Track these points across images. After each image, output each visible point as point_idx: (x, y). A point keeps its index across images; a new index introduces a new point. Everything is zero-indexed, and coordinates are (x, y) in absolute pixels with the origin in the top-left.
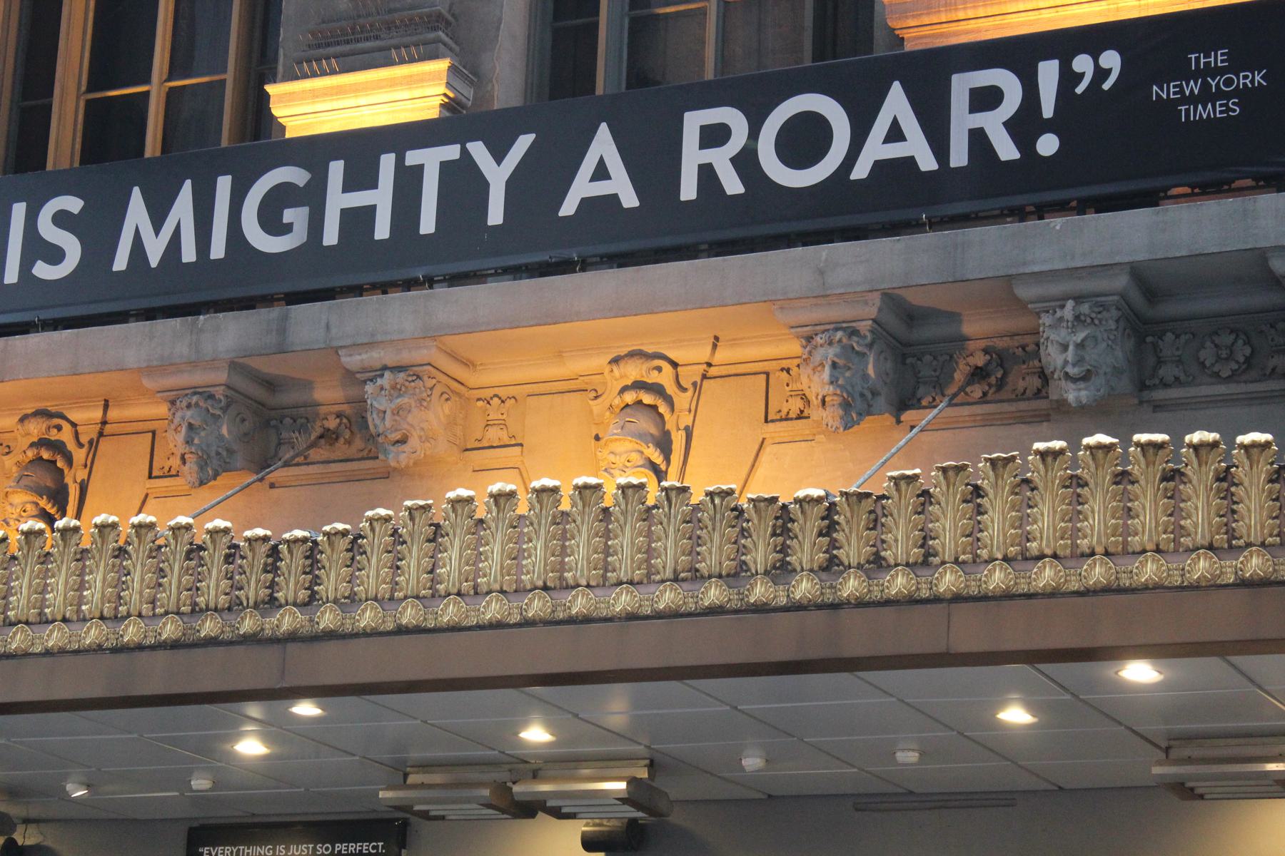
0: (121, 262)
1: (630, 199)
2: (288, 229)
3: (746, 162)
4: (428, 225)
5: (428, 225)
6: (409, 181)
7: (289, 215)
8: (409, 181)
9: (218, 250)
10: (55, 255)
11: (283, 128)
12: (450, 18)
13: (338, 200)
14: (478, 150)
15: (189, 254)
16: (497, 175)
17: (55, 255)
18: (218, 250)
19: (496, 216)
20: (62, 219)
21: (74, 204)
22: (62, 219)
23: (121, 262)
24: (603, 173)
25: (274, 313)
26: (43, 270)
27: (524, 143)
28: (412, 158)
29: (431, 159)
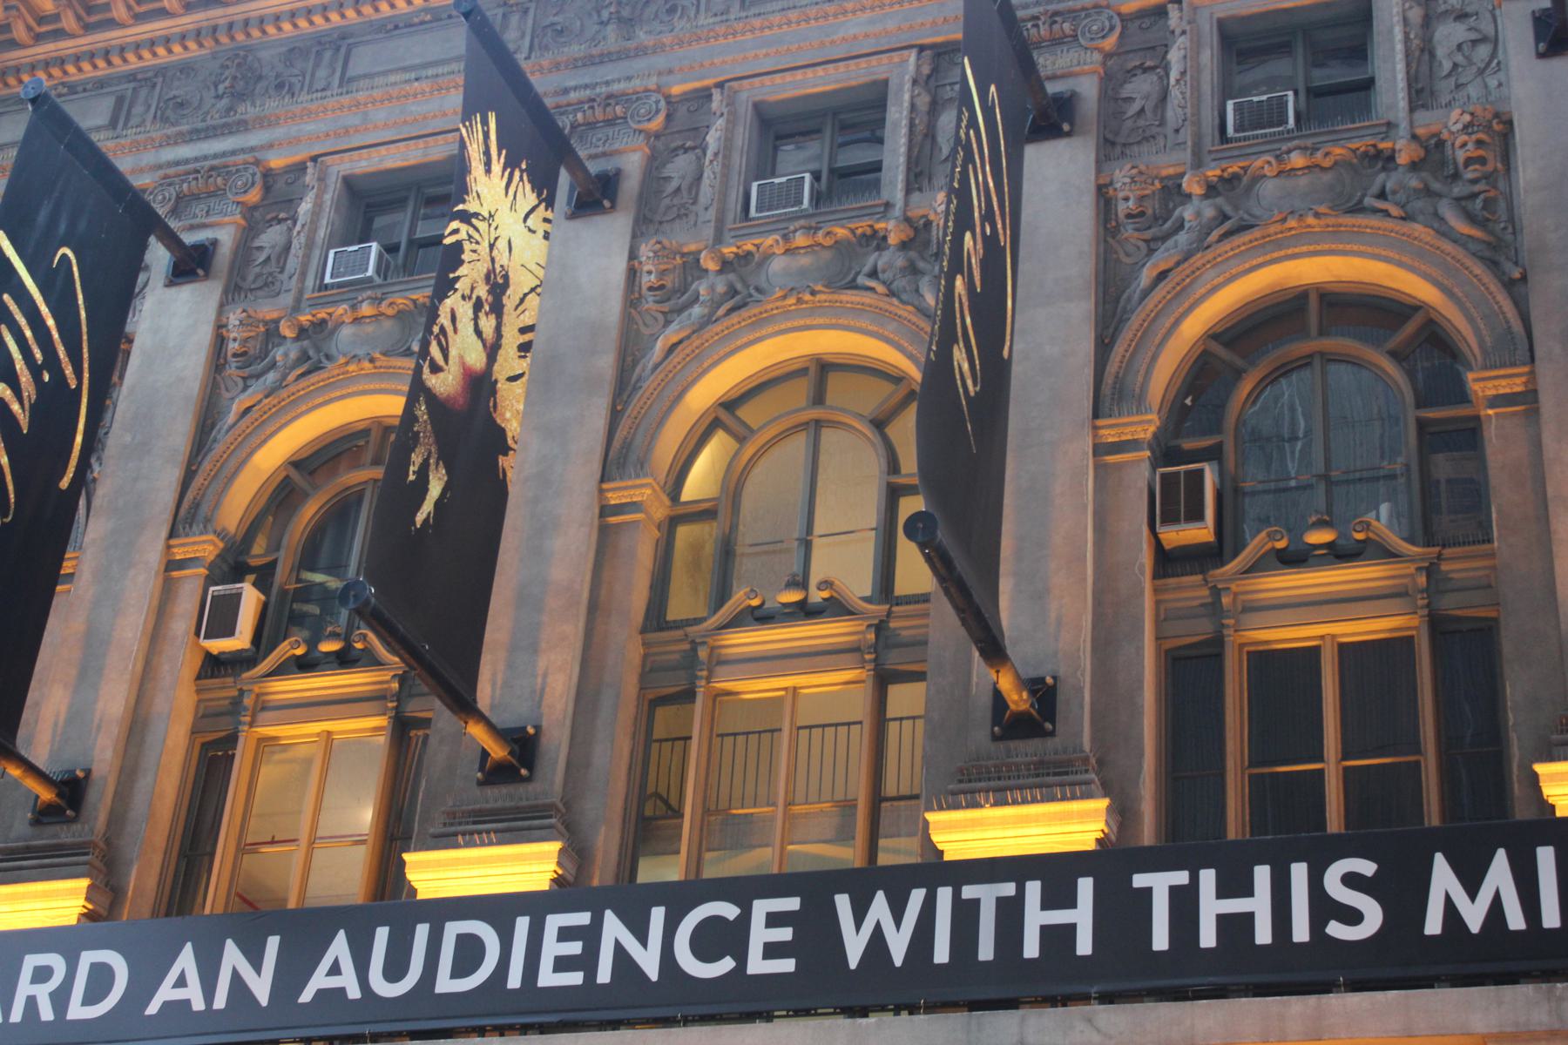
11: (414, 891)
12: (560, 806)
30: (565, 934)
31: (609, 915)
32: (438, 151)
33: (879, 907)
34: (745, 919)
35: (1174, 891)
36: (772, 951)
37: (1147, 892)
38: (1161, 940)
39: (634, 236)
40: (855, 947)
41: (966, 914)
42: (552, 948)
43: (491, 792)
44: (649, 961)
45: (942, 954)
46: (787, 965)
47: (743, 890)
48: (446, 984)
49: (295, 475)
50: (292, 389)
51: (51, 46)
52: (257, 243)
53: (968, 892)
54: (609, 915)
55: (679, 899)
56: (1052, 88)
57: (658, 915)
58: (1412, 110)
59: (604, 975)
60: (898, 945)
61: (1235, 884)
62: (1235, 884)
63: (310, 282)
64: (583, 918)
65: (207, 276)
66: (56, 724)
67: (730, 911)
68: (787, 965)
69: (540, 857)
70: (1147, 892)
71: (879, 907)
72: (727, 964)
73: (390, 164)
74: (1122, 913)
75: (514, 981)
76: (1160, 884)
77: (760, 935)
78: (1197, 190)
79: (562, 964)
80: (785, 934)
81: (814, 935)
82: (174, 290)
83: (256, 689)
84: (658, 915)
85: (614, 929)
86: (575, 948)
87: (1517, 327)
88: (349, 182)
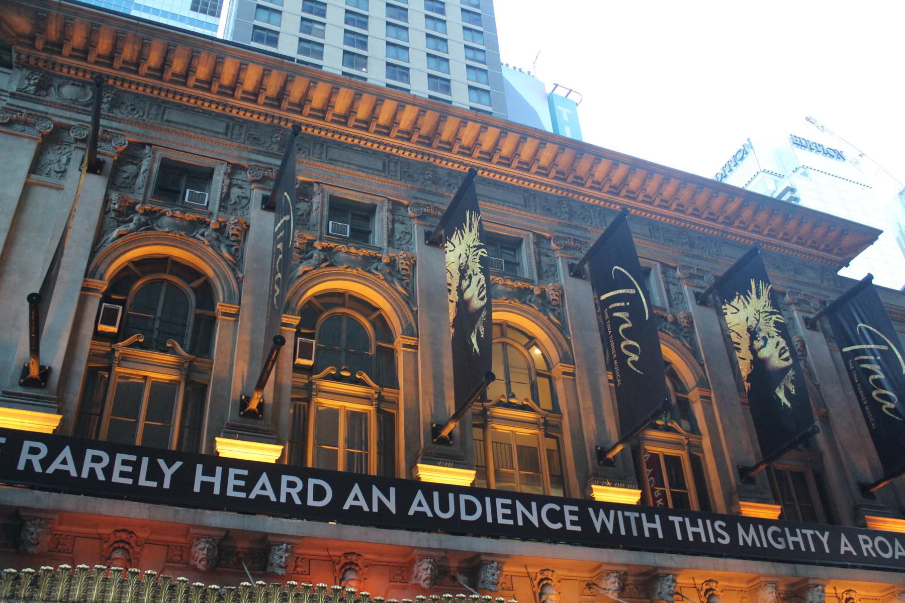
0: (741, 543)
1: (855, 553)
2: (779, 543)
3: (873, 548)
4: (813, 550)
5: (813, 550)
6: (804, 537)
7: (780, 539)
8: (804, 537)
9: (765, 545)
10: (723, 538)
13: (791, 539)
14: (817, 532)
15: (758, 545)
16: (824, 540)
17: (723, 538)
18: (765, 545)
19: (827, 551)
20: (720, 527)
21: (724, 524)
22: (720, 527)
23: (741, 543)
24: (845, 546)
25: (792, 565)
26: (720, 540)
27: (827, 534)
28: (804, 531)
29: (809, 532)
30: (504, 506)
31: (517, 501)
32: (367, 200)
33: (602, 514)
34: (562, 510)
35: (680, 522)
36: (573, 523)
37: (673, 522)
38: (680, 537)
39: (107, 188)
40: (598, 526)
41: (627, 520)
42: (500, 511)
43: (438, 447)
44: (534, 520)
45: (623, 532)
46: (578, 529)
47: (560, 501)
48: (464, 517)
49: (131, 266)
50: (321, 271)
51: (200, 92)
52: (122, 169)
53: (626, 514)
54: (517, 501)
55: (542, 500)
56: (99, 156)
57: (534, 505)
58: (219, 210)
59: (520, 523)
60: (610, 527)
61: (694, 524)
62: (694, 524)
63: (324, 231)
64: (509, 502)
65: (99, 174)
66: (243, 376)
67: (558, 508)
68: (578, 529)
69: (469, 475)
70: (673, 522)
71: (602, 514)
72: (558, 526)
73: (348, 197)
74: (668, 527)
75: (489, 519)
76: (676, 520)
77: (568, 518)
78: (320, 248)
79: (505, 516)
80: (576, 518)
81: (584, 520)
82: (265, 213)
83: (318, 383)
84: (534, 505)
85: (520, 507)
86: (508, 511)
87: (414, 325)
88: (331, 196)
